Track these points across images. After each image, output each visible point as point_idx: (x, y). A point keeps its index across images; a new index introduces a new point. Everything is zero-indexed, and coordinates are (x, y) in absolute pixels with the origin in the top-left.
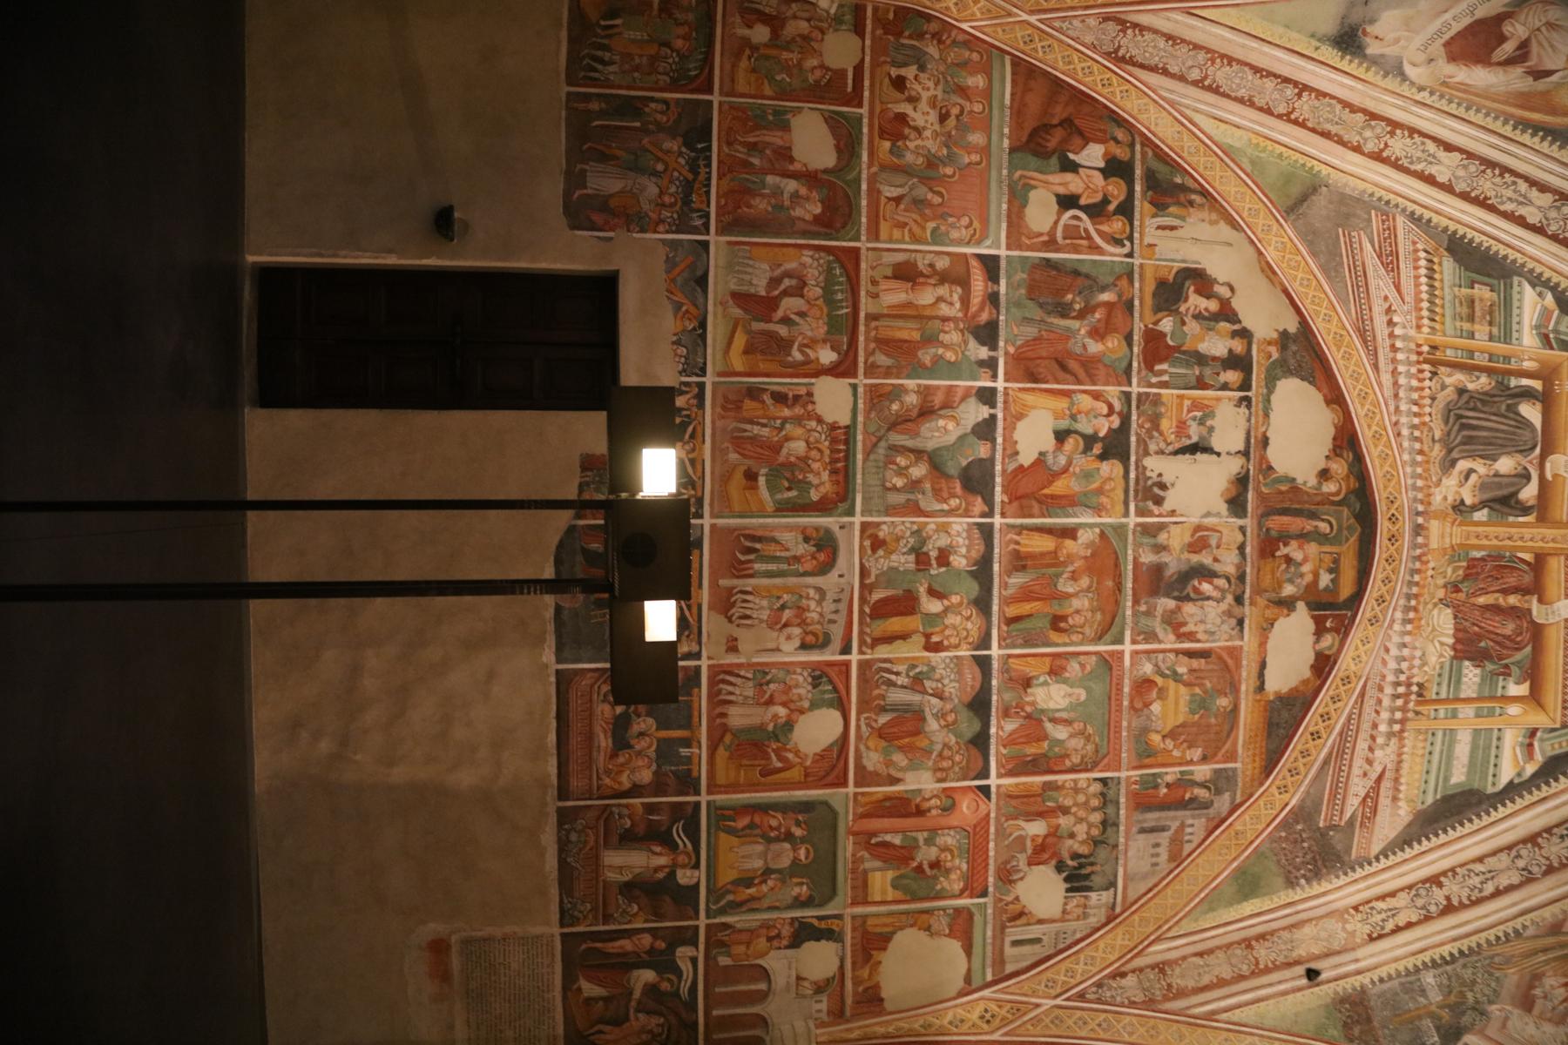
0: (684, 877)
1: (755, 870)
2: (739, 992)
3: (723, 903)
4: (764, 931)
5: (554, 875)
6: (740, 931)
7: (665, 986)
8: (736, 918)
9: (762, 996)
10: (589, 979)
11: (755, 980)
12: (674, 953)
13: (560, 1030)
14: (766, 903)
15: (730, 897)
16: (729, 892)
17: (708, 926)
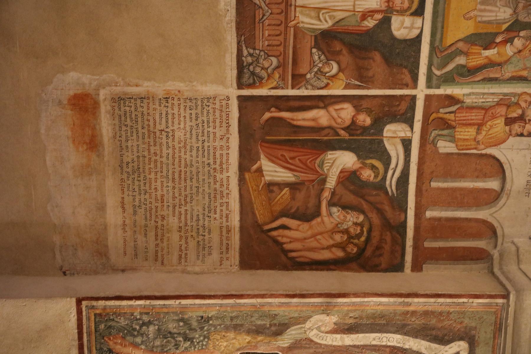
0: (402, 27)
1: (499, 23)
2: (461, 189)
3: (450, 67)
4: (502, 110)
5: (231, 15)
6: (471, 108)
7: (367, 174)
8: (466, 90)
9: (493, 198)
10: (272, 159)
11: (485, 176)
12: (382, 130)
13: (235, 220)
14: (509, 71)
15: (461, 60)
16: (460, 52)
17: (428, 98)
